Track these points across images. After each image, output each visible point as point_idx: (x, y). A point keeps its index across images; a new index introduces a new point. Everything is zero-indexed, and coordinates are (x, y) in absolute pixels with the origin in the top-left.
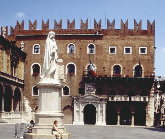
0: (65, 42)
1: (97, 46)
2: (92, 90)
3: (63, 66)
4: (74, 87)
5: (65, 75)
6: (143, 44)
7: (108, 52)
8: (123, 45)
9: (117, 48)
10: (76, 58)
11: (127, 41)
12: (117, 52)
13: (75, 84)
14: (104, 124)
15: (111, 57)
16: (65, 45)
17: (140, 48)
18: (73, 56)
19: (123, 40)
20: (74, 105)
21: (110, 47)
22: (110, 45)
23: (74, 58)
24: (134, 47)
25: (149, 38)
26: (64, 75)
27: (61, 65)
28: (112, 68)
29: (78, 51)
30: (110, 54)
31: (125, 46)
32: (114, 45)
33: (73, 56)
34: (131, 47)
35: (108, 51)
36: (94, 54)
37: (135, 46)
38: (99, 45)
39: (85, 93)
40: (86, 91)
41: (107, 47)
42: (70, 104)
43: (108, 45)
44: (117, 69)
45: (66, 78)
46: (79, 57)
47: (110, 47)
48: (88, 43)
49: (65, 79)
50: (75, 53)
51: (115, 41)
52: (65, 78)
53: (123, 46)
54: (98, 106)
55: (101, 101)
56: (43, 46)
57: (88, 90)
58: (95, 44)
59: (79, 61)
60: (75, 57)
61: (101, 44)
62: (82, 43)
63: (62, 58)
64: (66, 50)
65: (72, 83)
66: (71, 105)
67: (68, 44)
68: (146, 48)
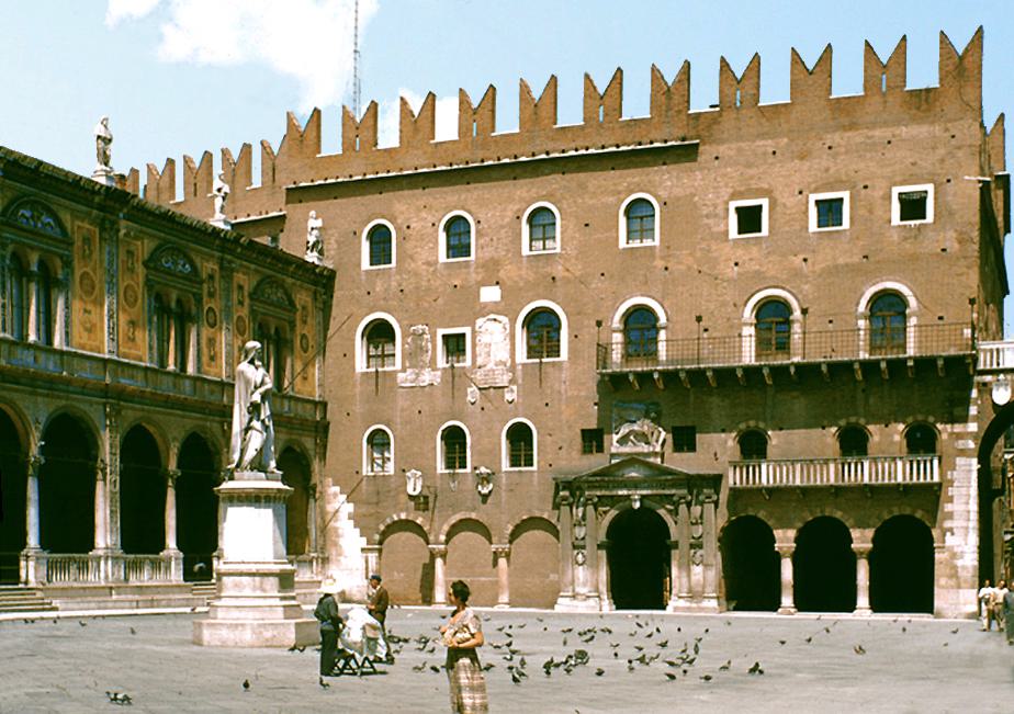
0: (510, 200)
3: (505, 320)
6: (915, 170)
11: (825, 161)
15: (740, 254)
16: (510, 214)
17: (896, 191)
18: (549, 269)
21: (733, 205)
22: (734, 196)
24: (864, 191)
25: (947, 130)
27: (492, 316)
28: (748, 313)
30: (735, 240)
31: (816, 190)
34: (845, 195)
35: (722, 228)
36: (652, 248)
37: (866, 187)
38: (679, 199)
41: (720, 210)
43: (725, 192)
44: (773, 316)
45: (520, 381)
48: (619, 193)
49: (515, 388)
50: (558, 250)
56: (408, 227)
63: (498, 283)
67: (524, 205)
68: (930, 188)
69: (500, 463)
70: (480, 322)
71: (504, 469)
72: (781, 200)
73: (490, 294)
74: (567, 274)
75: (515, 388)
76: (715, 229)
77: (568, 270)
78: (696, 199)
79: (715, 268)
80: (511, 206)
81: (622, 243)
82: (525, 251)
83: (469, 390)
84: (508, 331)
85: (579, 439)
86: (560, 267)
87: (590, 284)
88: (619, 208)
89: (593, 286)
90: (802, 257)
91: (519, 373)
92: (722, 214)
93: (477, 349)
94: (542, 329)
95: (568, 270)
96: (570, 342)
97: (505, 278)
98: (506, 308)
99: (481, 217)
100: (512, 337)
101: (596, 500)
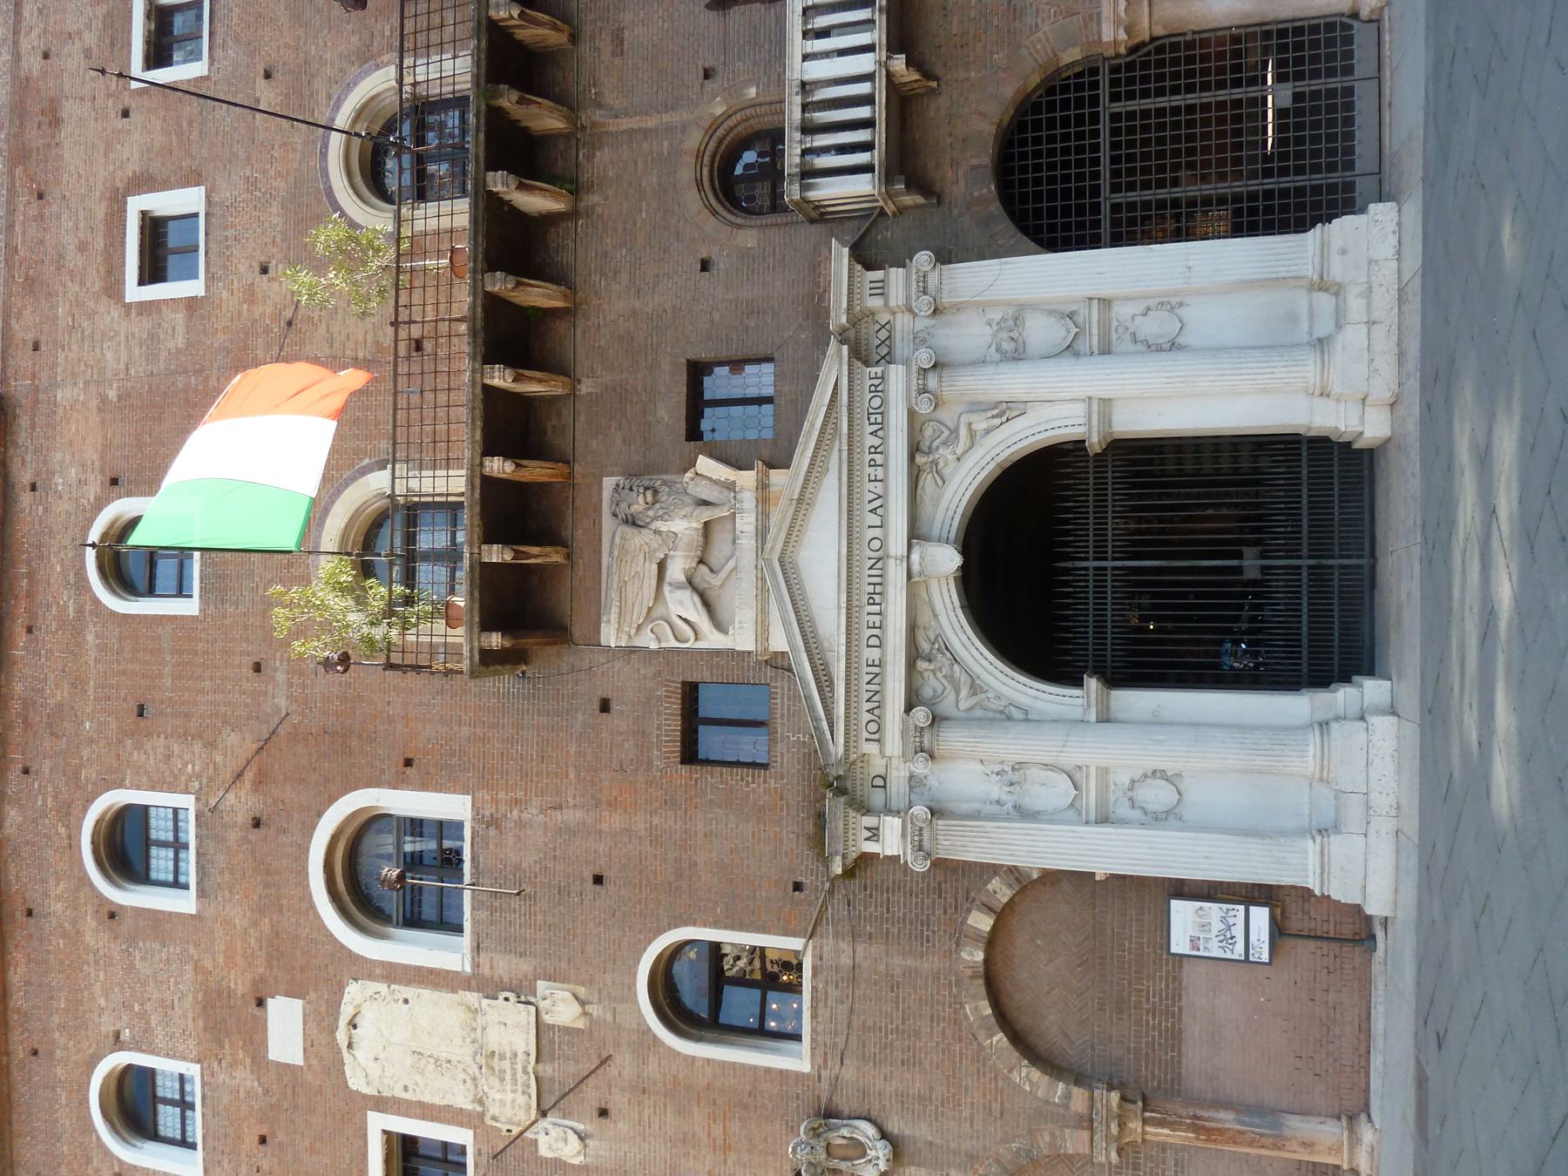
0: (74, 938)
1: (114, 482)
5: (489, 987)
7: (191, 304)
8: (113, 108)
9: (145, 183)
10: (260, 782)
11: (72, 60)
12: (190, 178)
13: (614, 821)
14: (1368, 247)
15: (245, 269)
18: (233, 836)
19: (56, 122)
22: (114, 289)
23: (257, 823)
26: (472, 998)
27: (341, 1036)
29: (168, 757)
32: (109, 234)
33: (233, 836)
35: (180, 318)
38: (107, 447)
39: (742, 639)
42: (960, 936)
43: (110, 316)
45: (525, 967)
46: (237, 744)
47: (134, 292)
48: (80, 610)
49: (541, 985)
51: (67, 224)
52: (522, 991)
53: (126, 114)
54: (1004, 410)
55: (901, 348)
58: (98, 507)
59: (294, 737)
60: (240, 803)
61: (95, 418)
62: (78, 684)
63: (260, 1003)
64: (157, 921)
65: (598, 880)
66: (982, 922)
69: (783, 1074)
70: (356, 1082)
71: (805, 1066)
72: (133, 167)
73: (285, 1028)
74: (249, 775)
75: (541, 985)
76: (180, 341)
77: (239, 776)
78: (112, 394)
79: (267, 331)
80: (89, 938)
81: (189, 607)
82: (184, 903)
83: (544, 1151)
84: (382, 987)
85: (711, 778)
86: (231, 797)
87: (277, 709)
88: (113, 614)
89: (282, 702)
90: (261, 82)
91: (503, 965)
92: (147, 323)
93: (427, 1098)
94: (397, 883)
95: (239, 776)
96: (424, 786)
97: (249, 976)
98: (321, 979)
99: (107, 1025)
100: (394, 974)
101: (921, 715)
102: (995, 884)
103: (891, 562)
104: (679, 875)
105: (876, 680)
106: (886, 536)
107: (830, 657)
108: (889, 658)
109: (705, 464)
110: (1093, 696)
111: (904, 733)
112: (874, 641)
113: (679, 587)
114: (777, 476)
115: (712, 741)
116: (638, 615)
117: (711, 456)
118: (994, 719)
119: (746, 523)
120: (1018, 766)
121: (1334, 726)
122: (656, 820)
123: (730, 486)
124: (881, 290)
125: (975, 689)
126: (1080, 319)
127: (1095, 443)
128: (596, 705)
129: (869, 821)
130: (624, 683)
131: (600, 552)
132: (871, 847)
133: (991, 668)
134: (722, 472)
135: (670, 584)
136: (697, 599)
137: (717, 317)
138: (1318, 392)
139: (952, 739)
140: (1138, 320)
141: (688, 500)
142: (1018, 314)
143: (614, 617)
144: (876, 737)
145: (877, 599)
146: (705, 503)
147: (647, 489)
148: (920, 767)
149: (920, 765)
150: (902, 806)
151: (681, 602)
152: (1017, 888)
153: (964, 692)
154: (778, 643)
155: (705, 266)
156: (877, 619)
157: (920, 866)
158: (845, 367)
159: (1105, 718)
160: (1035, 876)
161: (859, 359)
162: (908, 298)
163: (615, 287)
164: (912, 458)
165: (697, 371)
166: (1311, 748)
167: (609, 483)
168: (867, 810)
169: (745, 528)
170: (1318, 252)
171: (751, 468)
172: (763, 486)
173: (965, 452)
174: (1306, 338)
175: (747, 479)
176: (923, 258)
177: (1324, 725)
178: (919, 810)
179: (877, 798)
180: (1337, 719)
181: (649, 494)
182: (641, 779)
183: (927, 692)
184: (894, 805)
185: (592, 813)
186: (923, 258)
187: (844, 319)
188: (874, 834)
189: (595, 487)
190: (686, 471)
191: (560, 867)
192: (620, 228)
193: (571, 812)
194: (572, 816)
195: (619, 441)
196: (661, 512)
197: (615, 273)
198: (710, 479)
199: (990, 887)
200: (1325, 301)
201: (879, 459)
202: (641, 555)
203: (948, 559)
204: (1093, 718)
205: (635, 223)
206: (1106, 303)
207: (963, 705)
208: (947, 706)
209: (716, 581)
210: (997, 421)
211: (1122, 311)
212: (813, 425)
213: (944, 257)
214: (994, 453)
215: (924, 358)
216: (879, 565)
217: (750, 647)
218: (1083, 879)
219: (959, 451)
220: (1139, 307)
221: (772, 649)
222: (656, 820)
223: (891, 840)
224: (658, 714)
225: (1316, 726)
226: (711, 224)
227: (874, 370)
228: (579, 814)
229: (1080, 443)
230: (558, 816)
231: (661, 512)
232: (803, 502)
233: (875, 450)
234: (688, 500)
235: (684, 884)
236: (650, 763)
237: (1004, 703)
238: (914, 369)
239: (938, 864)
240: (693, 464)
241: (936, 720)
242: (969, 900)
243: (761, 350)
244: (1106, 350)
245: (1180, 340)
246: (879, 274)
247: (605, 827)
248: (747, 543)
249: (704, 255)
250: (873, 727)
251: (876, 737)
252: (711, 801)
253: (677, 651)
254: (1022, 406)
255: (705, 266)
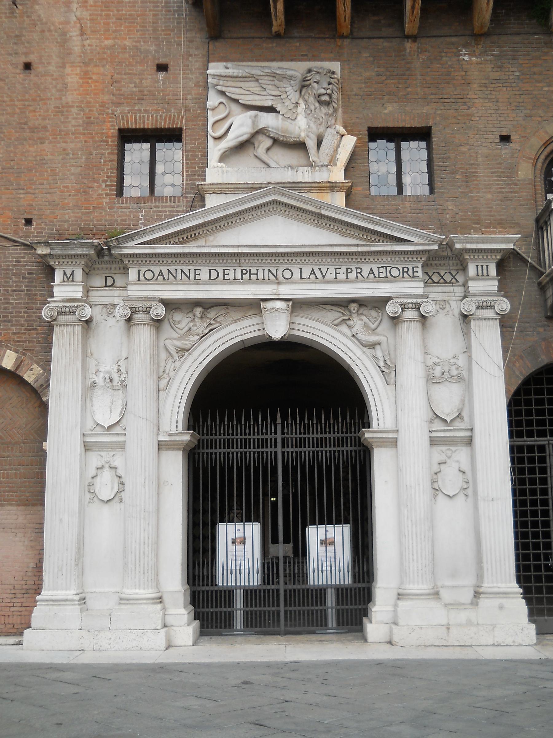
2: (300, 146)
4: (62, 110)
13: (73, 77)
14: (503, 626)
20: (46, 365)
40: (224, 157)
55: (437, 292)
57: (243, 146)
65: (28, 66)
85: (109, 152)
101: (160, 311)
102: (37, 370)
103: (274, 287)
104: (33, 130)
105: (184, 277)
106: (295, 283)
107: (201, 242)
108: (201, 287)
109: (350, 142)
110: (177, 438)
111: (146, 299)
112: (214, 275)
113: (254, 123)
114: (339, 199)
115: (137, 153)
116: (232, 92)
117: (355, 147)
118: (158, 366)
119: (305, 175)
120: (124, 386)
121: (159, 606)
122: (74, 110)
123: (332, 162)
124: (482, 275)
125: (183, 351)
126: (458, 425)
127: (368, 435)
128: (162, 61)
129: (79, 274)
130: (180, 82)
131: (281, 60)
132: (58, 276)
133: (197, 363)
134: (343, 156)
135: (256, 116)
136: (245, 137)
137: (464, 149)
138: (401, 591)
139: (143, 334)
140: (455, 466)
141: (322, 129)
142: (464, 379)
143: (231, 71)
144: (142, 278)
145: (246, 277)
146: (319, 144)
147: (330, 96)
148: (121, 311)
149: (121, 312)
150: (91, 299)
151: (242, 125)
152: (35, 386)
153: (179, 343)
154: (212, 201)
155: (505, 139)
156: (231, 276)
157: (45, 313)
158: (420, 248)
159: (162, 446)
160: (44, 399)
161: (429, 259)
162: (474, 295)
163: (489, 68)
164: (353, 300)
165: (423, 134)
166: (142, 591)
167: (336, 66)
168: (87, 274)
169: (300, 173)
170: (501, 590)
171: (346, 176)
172: (332, 187)
173: (358, 340)
174: (439, 584)
175: (337, 175)
176: (504, 305)
177: (160, 600)
178: (87, 312)
179: (98, 281)
180: (164, 609)
181: (326, 98)
182: (106, 98)
183: (178, 316)
184: (92, 294)
185: (78, 59)
186: (504, 305)
187: (458, 246)
188: (69, 279)
189: (332, 55)
190: (345, 127)
191: (36, 36)
192: (535, 69)
193: (78, 43)
194: (76, 43)
195: (368, 74)
196: (313, 108)
197: (500, 67)
198: (338, 146)
199: (35, 366)
200: (467, 596)
201: (352, 276)
202: (278, 93)
203: (277, 329)
204: (161, 438)
205: (540, 82)
206: (469, 441)
207: (168, 342)
208: (167, 331)
209: (261, 150)
210: (382, 364)
211: (461, 455)
212: (377, 223)
213: (505, 322)
214: (358, 362)
215: (428, 308)
216: (272, 277)
217: (208, 180)
218: (42, 433)
219: (360, 336)
220: (465, 467)
221: (207, 196)
222: (74, 110)
223: (64, 291)
224: (157, 111)
225: (159, 595)
226: (536, 142)
227: (420, 270)
228: (77, 49)
229: (367, 424)
230: (74, 33)
231: (313, 108)
232: (319, 219)
233: (359, 272)
234: (322, 129)
235: (27, 134)
236: (119, 104)
237: (172, 374)
238: (420, 300)
239: (49, 328)
240: (350, 133)
241: (157, 323)
242: (23, 351)
243: (437, 184)
244: (433, 442)
245: (440, 496)
246: (493, 272)
247: (68, 70)
248: (289, 176)
249: (513, 138)
250: (149, 275)
251: (142, 278)
252: (91, 154)
253: (206, 125)
254: (392, 381)
255: (505, 139)
